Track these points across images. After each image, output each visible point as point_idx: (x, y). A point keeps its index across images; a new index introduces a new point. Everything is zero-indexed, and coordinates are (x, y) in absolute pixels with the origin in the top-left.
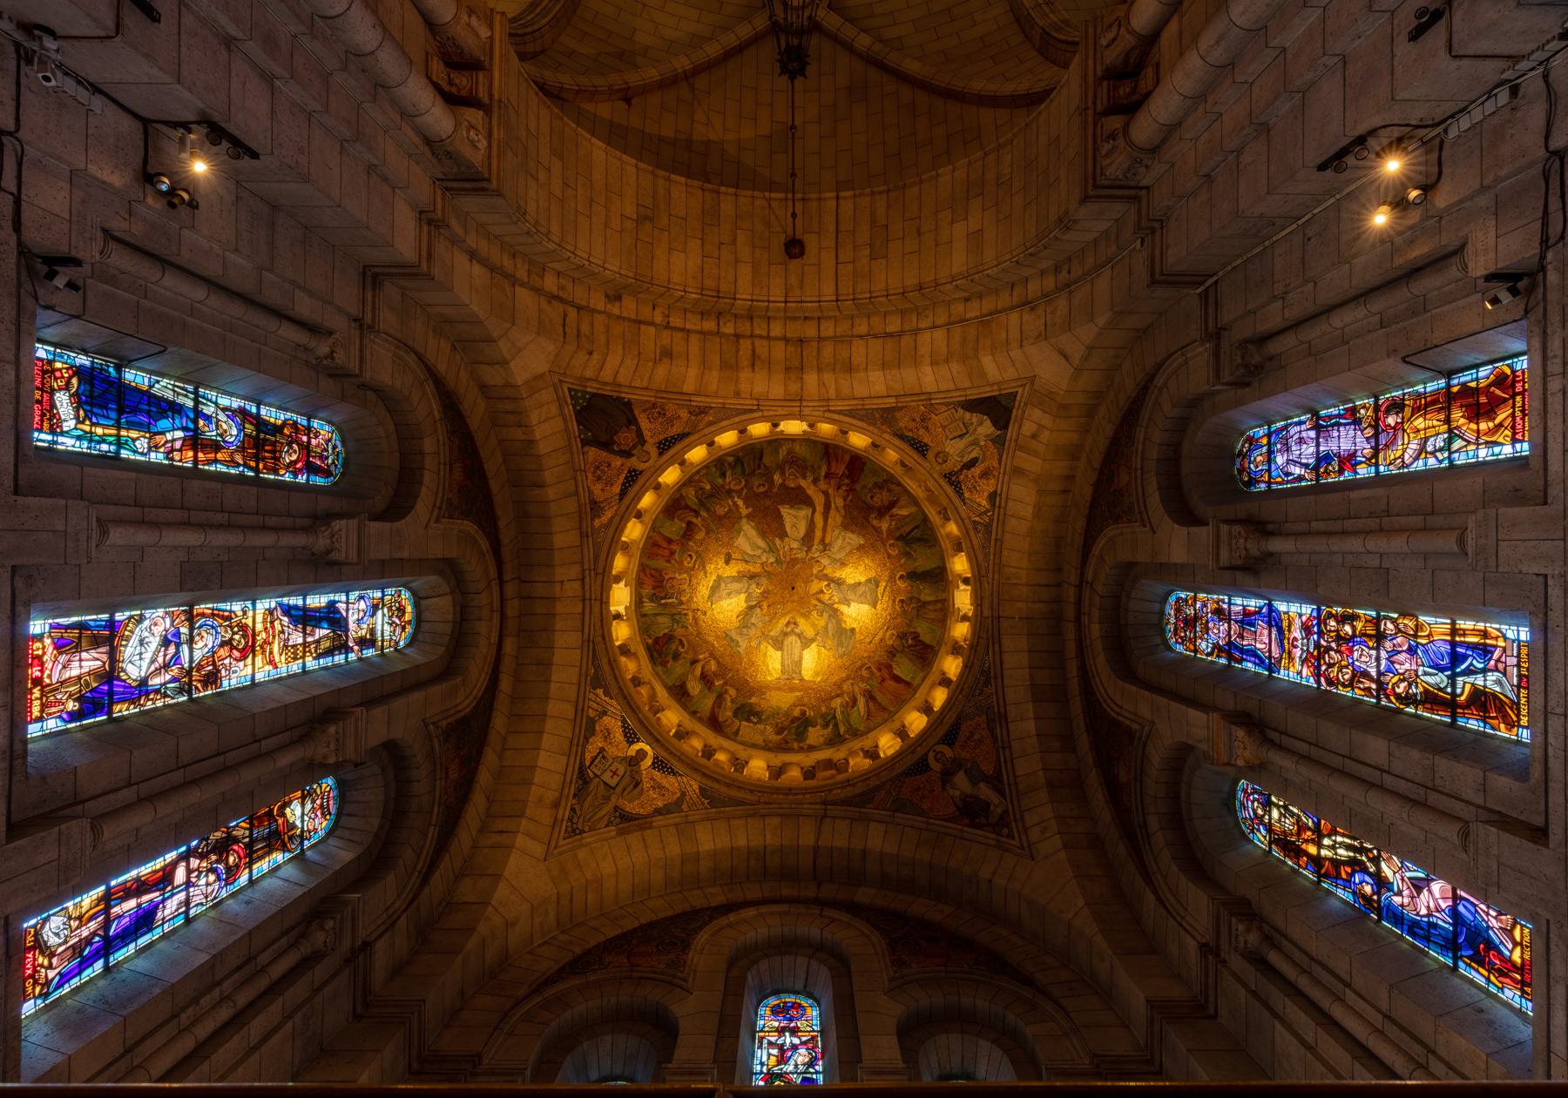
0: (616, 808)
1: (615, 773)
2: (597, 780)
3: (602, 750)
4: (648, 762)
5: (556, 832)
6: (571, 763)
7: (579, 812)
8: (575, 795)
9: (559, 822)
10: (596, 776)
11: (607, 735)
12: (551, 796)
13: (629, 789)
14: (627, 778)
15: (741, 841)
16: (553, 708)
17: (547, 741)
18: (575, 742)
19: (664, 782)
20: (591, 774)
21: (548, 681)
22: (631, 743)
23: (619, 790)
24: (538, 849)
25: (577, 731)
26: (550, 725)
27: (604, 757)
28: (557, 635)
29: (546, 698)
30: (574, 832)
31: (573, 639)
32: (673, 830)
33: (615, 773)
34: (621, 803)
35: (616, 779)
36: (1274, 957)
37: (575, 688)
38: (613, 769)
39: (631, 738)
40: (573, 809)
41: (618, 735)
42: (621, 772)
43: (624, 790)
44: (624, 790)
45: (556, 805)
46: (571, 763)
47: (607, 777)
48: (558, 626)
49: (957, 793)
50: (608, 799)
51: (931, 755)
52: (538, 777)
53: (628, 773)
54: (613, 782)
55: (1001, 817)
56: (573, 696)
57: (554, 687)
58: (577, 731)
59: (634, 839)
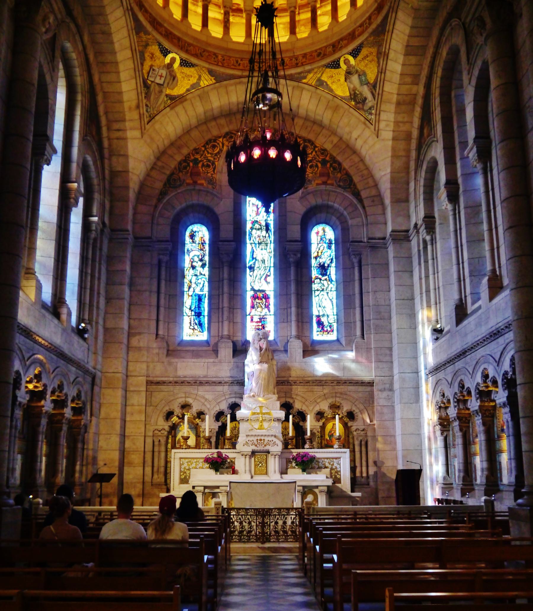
0: (167, 96)
1: (161, 76)
2: (153, 84)
3: (151, 66)
4: (176, 65)
5: (143, 122)
6: (138, 81)
7: (149, 105)
8: (145, 97)
9: (142, 116)
10: (152, 82)
11: (152, 56)
12: (134, 103)
13: (171, 82)
14: (168, 77)
15: (234, 99)
16: (120, 57)
17: (124, 76)
18: (137, 69)
19: (188, 73)
20: (149, 82)
21: (112, 43)
22: (165, 56)
23: (165, 85)
24: (137, 133)
25: (136, 62)
26: (121, 67)
27: (153, 70)
28: (109, 17)
29: (114, 53)
30: (152, 118)
31: (119, 13)
32: (198, 99)
33: (161, 76)
34: (168, 92)
35: (163, 79)
36: (429, 247)
37: (128, 39)
38: (160, 74)
39: (165, 52)
40: (147, 105)
41: (158, 53)
42: (164, 75)
43: (168, 84)
44: (168, 84)
45: (138, 107)
46: (138, 81)
47: (158, 81)
48: (108, 12)
49: (352, 86)
50: (161, 92)
51: (342, 59)
52: (125, 97)
53: (168, 73)
54: (161, 82)
55: (370, 108)
56: (128, 44)
57: (117, 46)
58: (136, 62)
59: (179, 109)
